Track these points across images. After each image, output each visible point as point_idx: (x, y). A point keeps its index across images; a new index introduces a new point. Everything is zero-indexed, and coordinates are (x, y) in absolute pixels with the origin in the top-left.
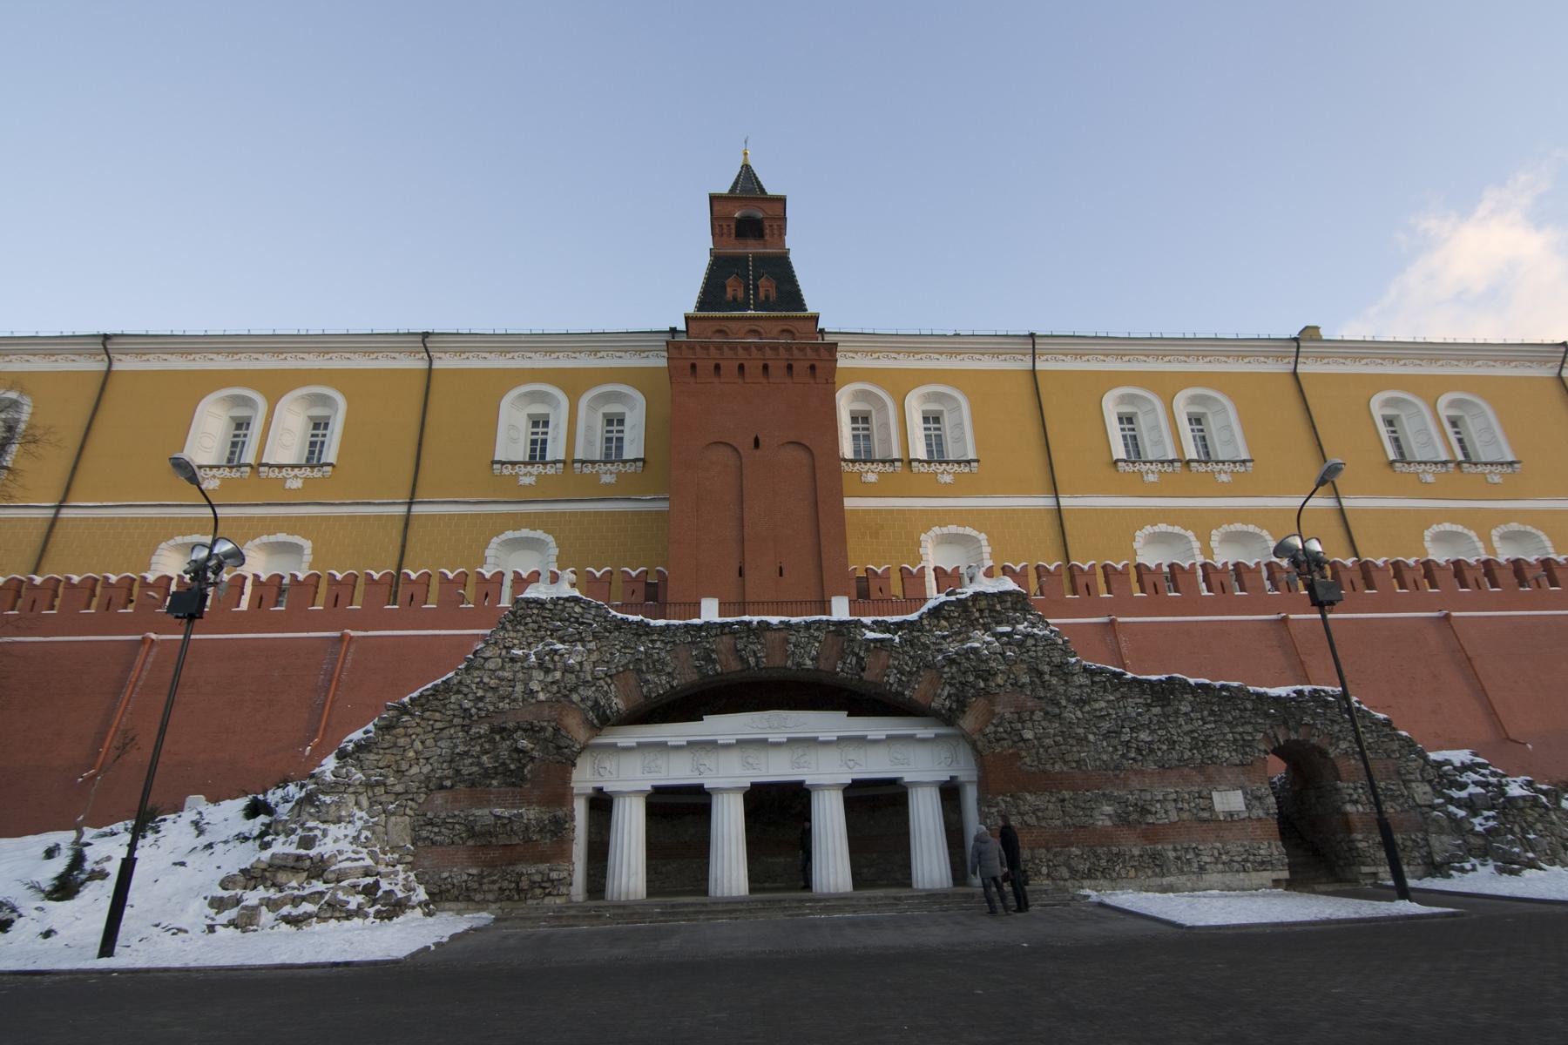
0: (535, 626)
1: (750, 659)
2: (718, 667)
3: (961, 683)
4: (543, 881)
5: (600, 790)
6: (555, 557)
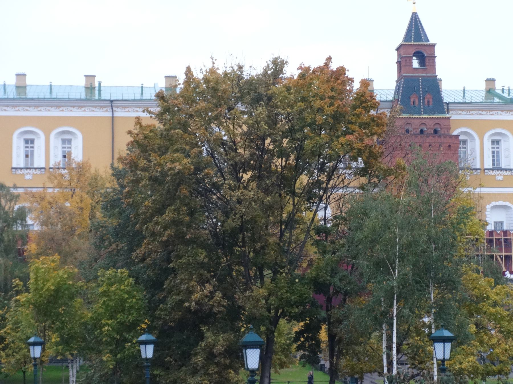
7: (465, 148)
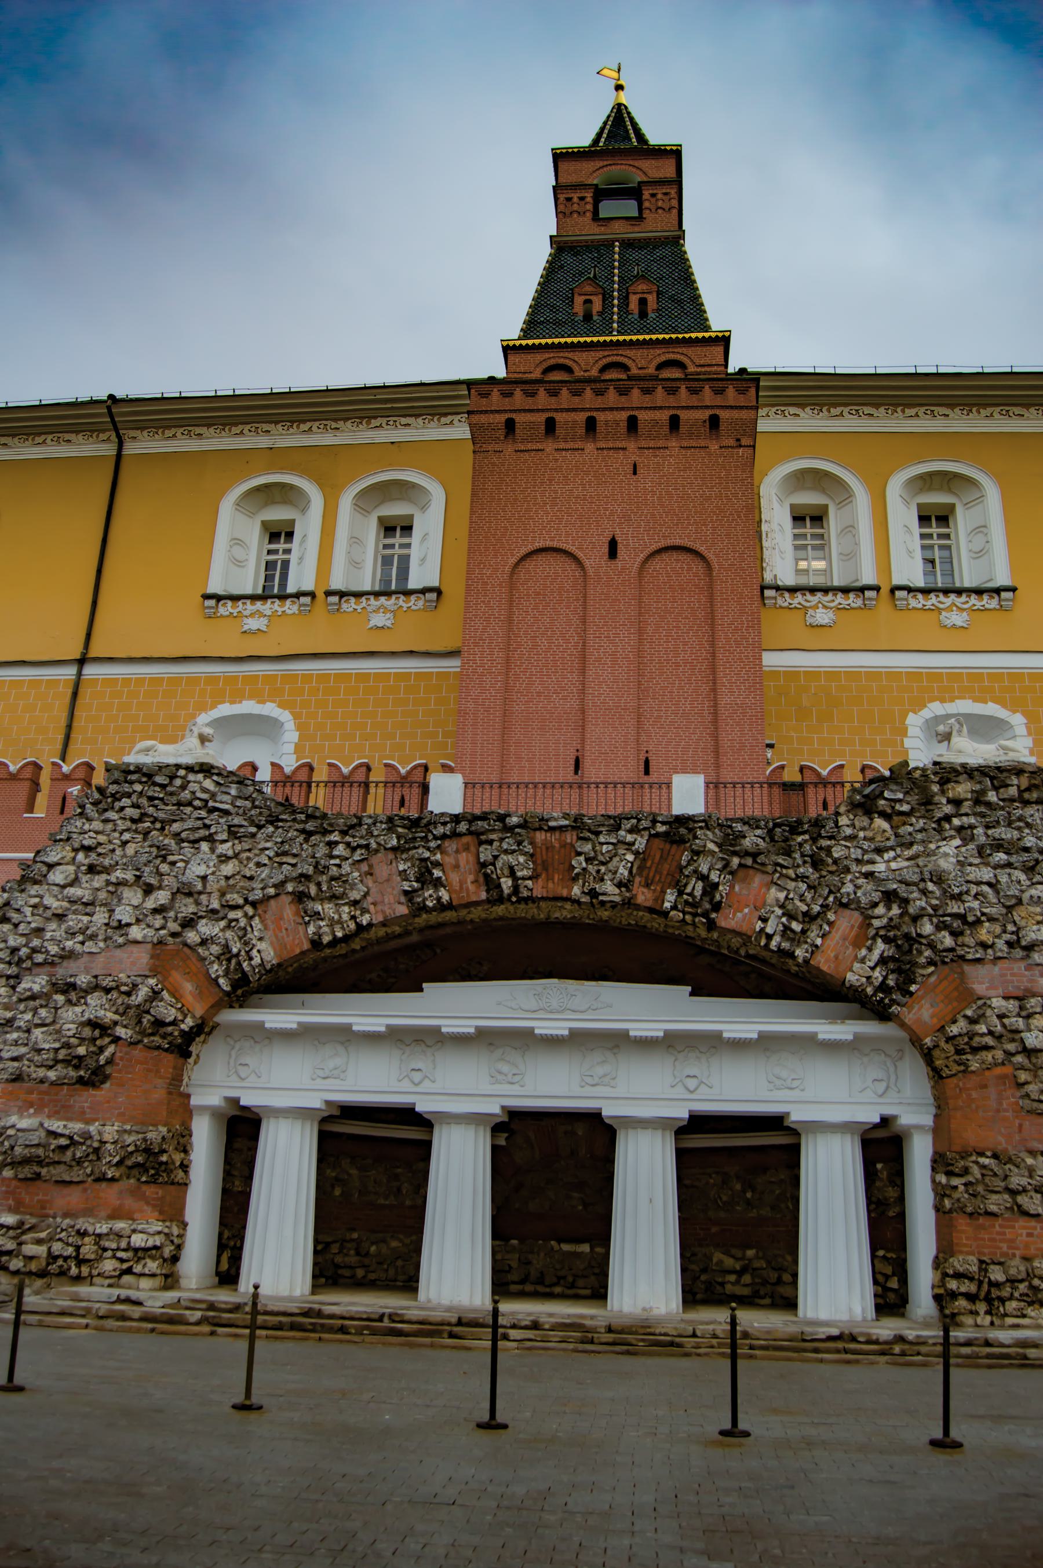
0: (134, 813)
1: (503, 880)
2: (443, 893)
3: (907, 936)
4: (118, 1249)
5: (234, 1101)
6: (293, 745)
7: (821, 536)
